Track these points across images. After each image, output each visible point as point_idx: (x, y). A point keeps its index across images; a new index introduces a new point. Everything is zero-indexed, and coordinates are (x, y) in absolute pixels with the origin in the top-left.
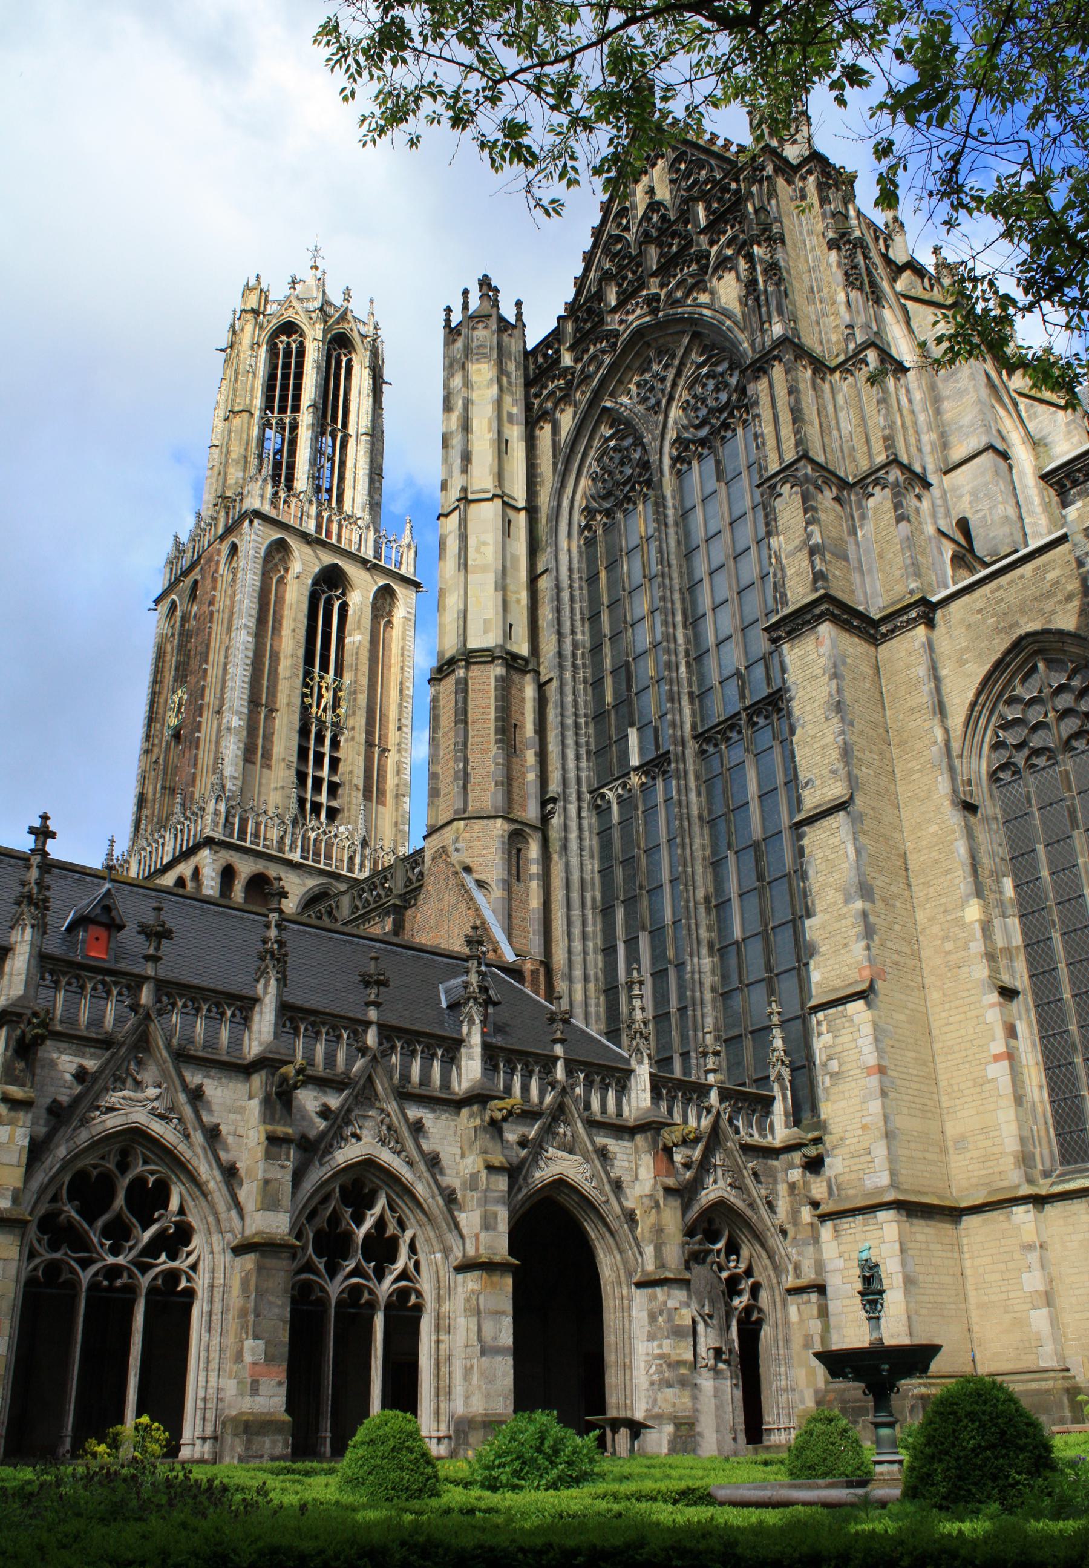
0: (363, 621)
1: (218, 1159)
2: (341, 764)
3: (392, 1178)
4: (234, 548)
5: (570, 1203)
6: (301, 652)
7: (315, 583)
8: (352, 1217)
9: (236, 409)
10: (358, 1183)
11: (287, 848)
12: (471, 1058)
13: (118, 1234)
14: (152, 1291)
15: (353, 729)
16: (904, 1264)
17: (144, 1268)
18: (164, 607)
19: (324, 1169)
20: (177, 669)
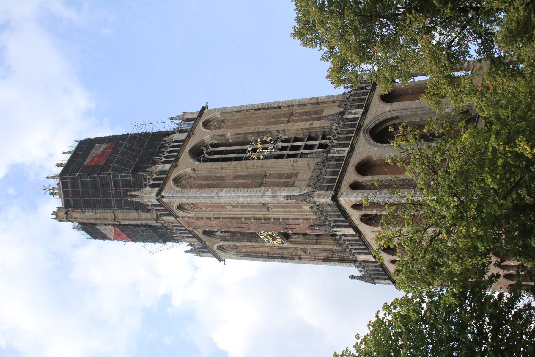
0: (220, 134)
2: (298, 136)
4: (180, 207)
6: (234, 163)
7: (199, 161)
9: (113, 218)
11: (342, 155)
15: (278, 131)
18: (221, 254)
20: (251, 241)
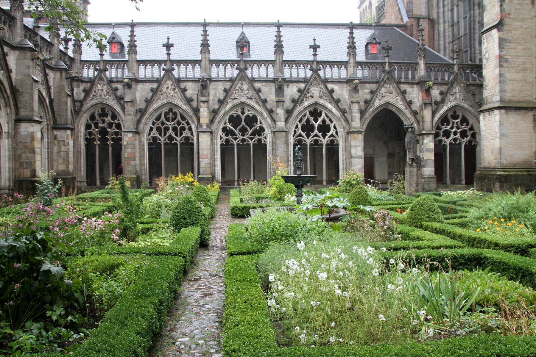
1: (267, 108)
3: (326, 108)
5: (394, 110)
8: (314, 120)
10: (316, 110)
12: (350, 67)
13: (243, 131)
14: (254, 145)
16: (500, 129)
17: (252, 139)
19: (301, 107)
